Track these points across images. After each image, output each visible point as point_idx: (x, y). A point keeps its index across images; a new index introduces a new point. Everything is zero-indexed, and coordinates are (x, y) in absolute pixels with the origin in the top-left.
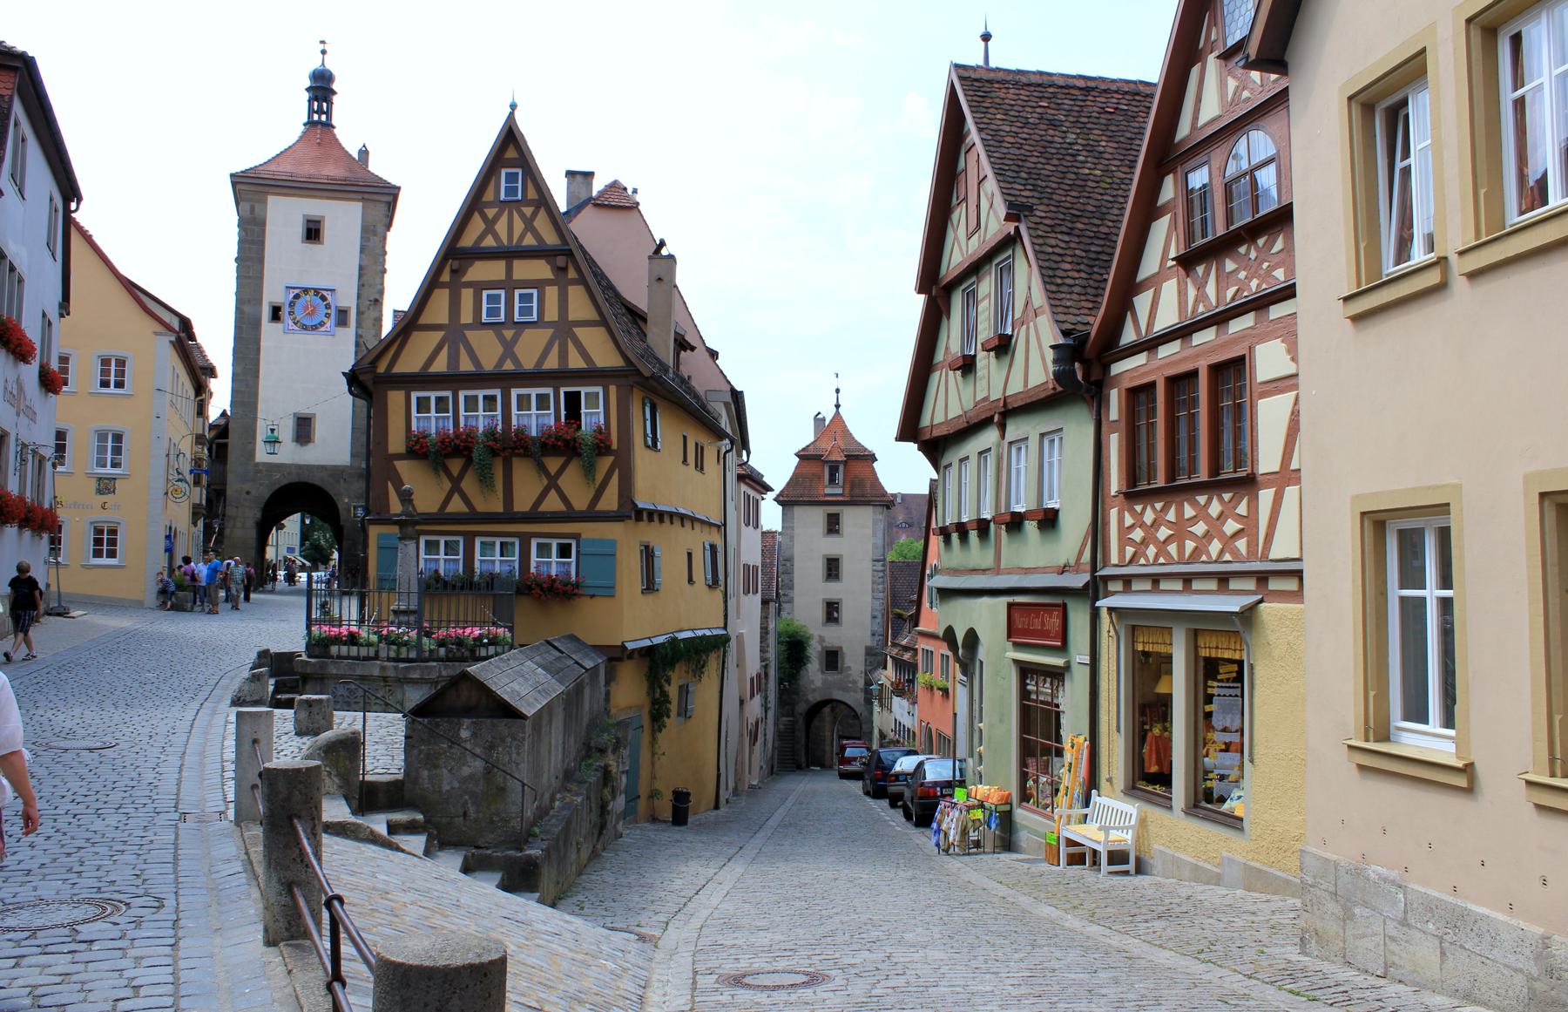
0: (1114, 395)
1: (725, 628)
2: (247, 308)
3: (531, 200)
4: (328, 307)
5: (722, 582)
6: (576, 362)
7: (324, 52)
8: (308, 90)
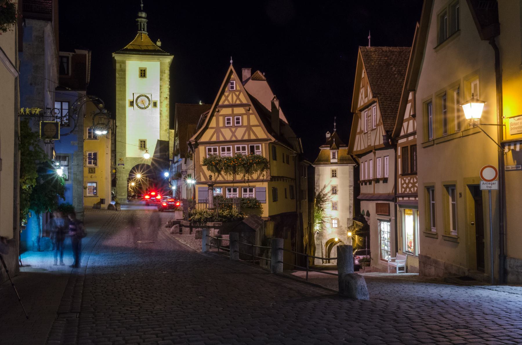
0: (399, 149)
4: (149, 101)
5: (295, 197)
6: (253, 137)
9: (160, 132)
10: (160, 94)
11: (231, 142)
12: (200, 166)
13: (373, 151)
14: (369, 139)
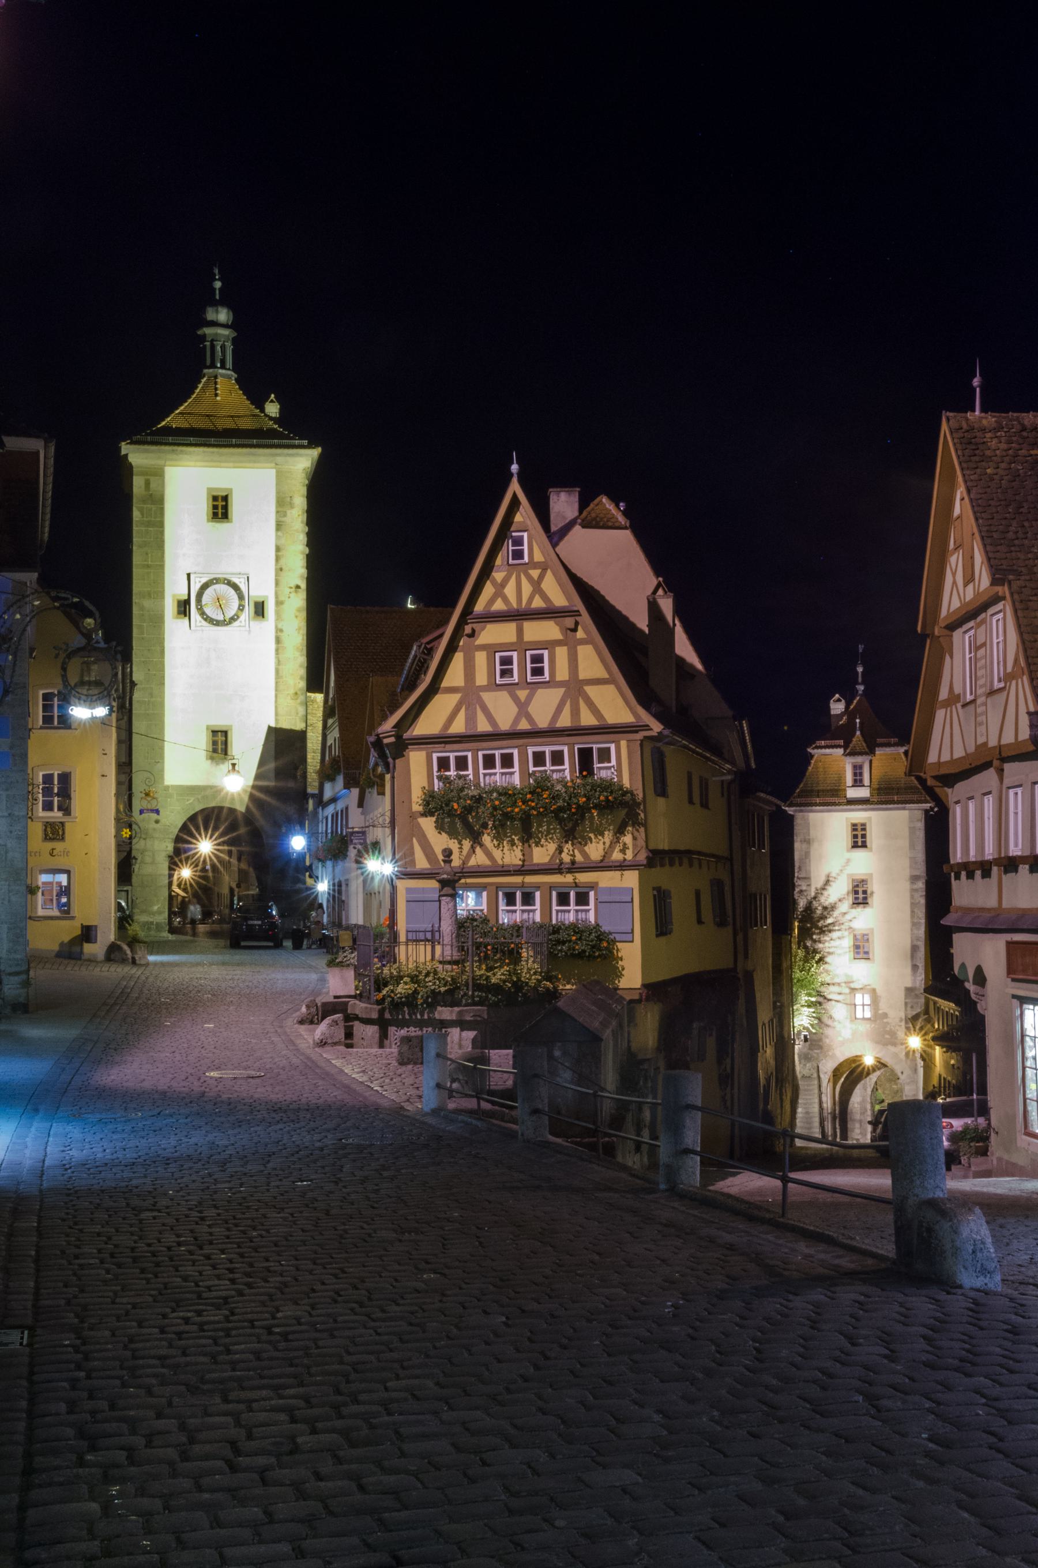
5: (730, 920)
6: (587, 719)
9: (276, 701)
10: (277, 575)
11: (514, 735)
13: (996, 763)
14: (981, 724)
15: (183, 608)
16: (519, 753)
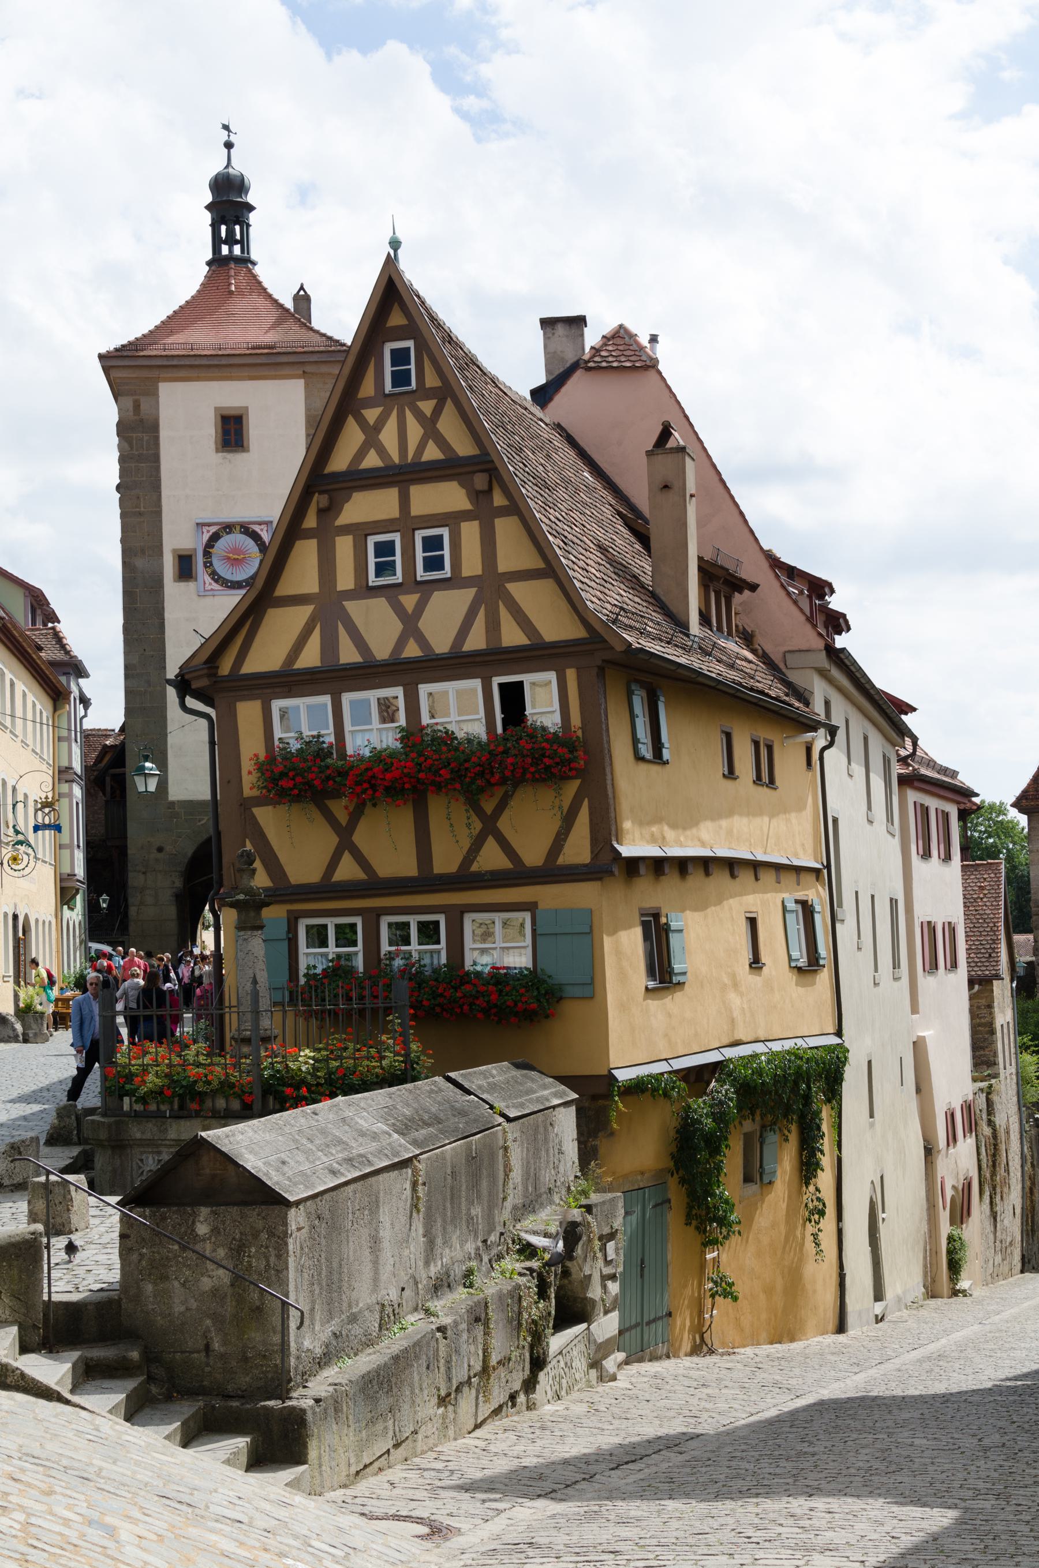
1: (839, 1033)
2: (139, 563)
3: (431, 388)
6: (512, 636)
7: (229, 145)
8: (208, 207)
12: (246, 805)
15: (185, 568)
16: (405, 696)
